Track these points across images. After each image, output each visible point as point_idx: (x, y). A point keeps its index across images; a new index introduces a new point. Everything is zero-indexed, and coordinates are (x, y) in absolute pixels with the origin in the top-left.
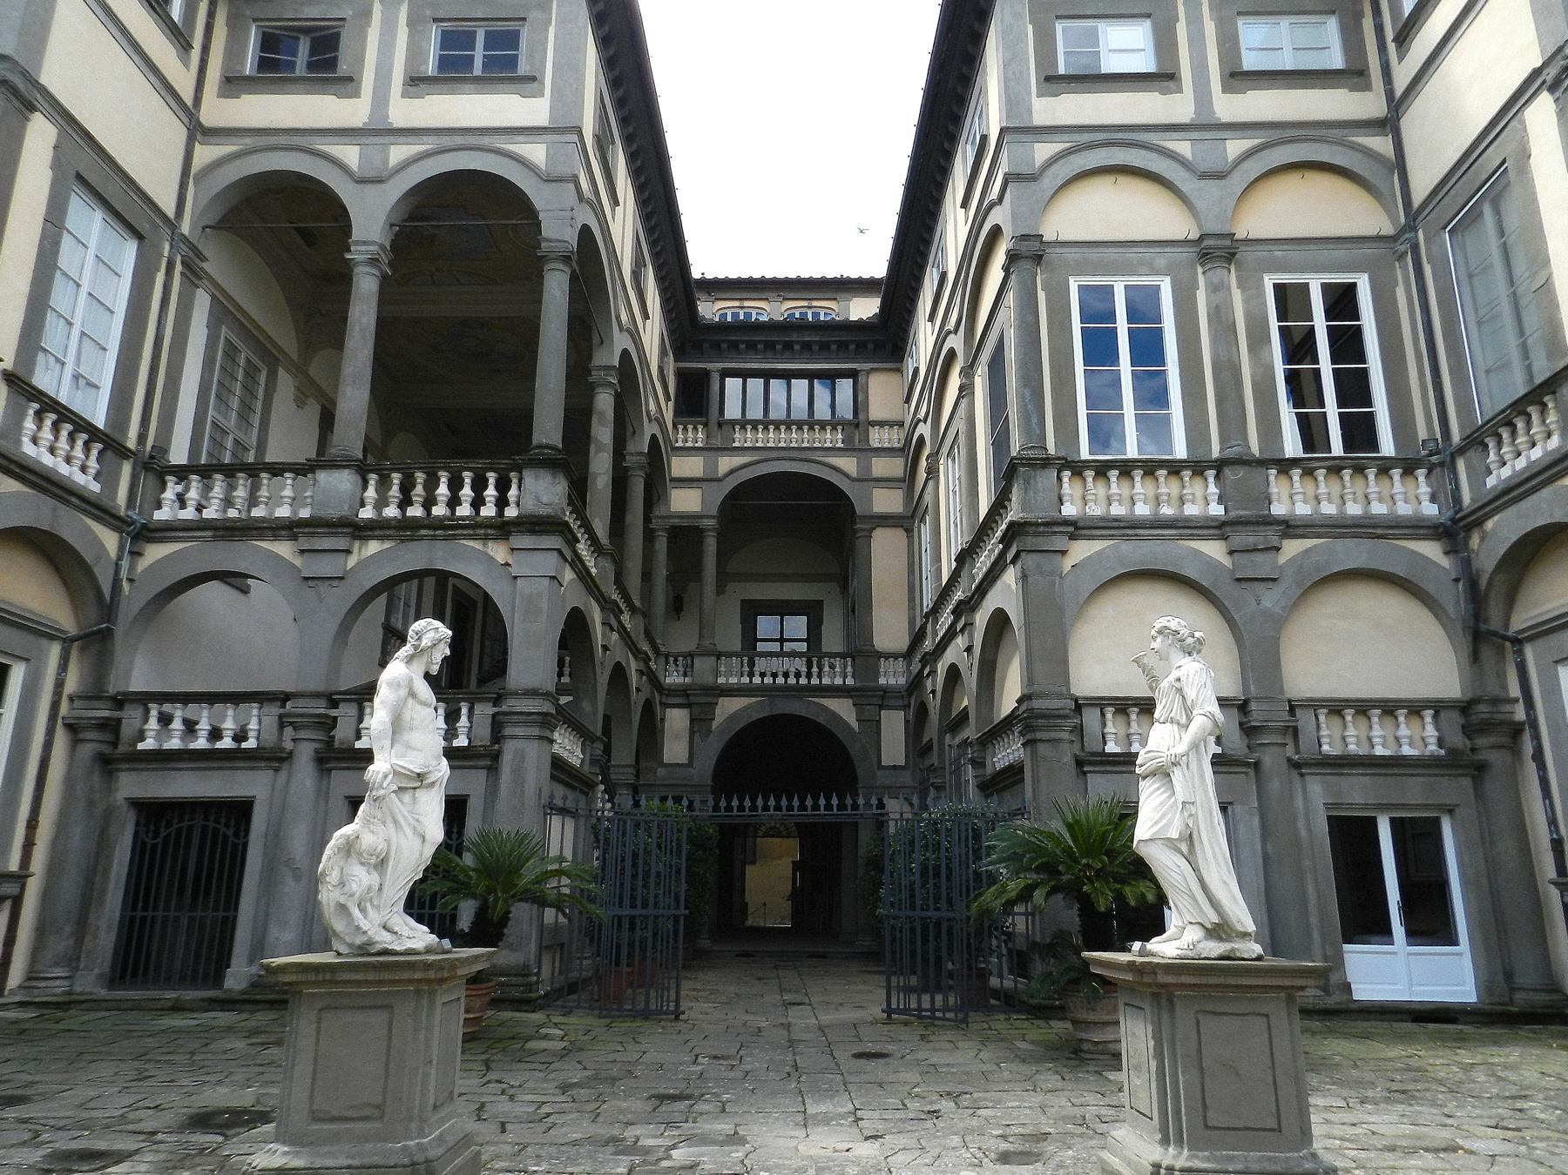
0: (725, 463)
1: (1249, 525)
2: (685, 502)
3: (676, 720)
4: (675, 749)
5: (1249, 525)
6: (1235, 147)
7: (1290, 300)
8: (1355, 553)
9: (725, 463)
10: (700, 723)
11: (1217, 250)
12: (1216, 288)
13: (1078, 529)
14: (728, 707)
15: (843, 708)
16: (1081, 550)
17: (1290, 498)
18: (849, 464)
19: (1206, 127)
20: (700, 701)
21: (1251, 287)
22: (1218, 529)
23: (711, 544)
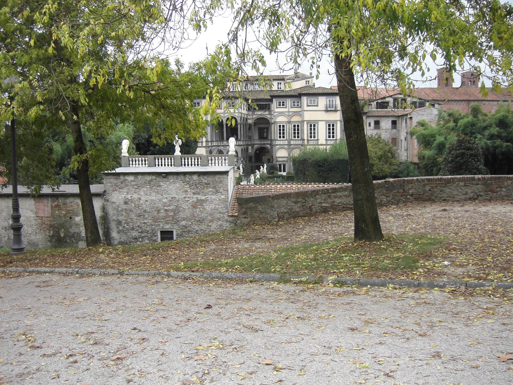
0: (254, 116)
1: (289, 145)
2: (250, 121)
3: (250, 147)
4: (250, 151)
5: (289, 145)
6: (291, 113)
7: (294, 126)
8: (296, 146)
9: (254, 116)
10: (253, 148)
11: (289, 122)
12: (289, 126)
13: (277, 145)
14: (256, 146)
15: (268, 146)
16: (277, 146)
17: (292, 142)
18: (269, 116)
19: (289, 112)
20: (252, 145)
21: (291, 125)
22: (286, 145)
23: (253, 127)
